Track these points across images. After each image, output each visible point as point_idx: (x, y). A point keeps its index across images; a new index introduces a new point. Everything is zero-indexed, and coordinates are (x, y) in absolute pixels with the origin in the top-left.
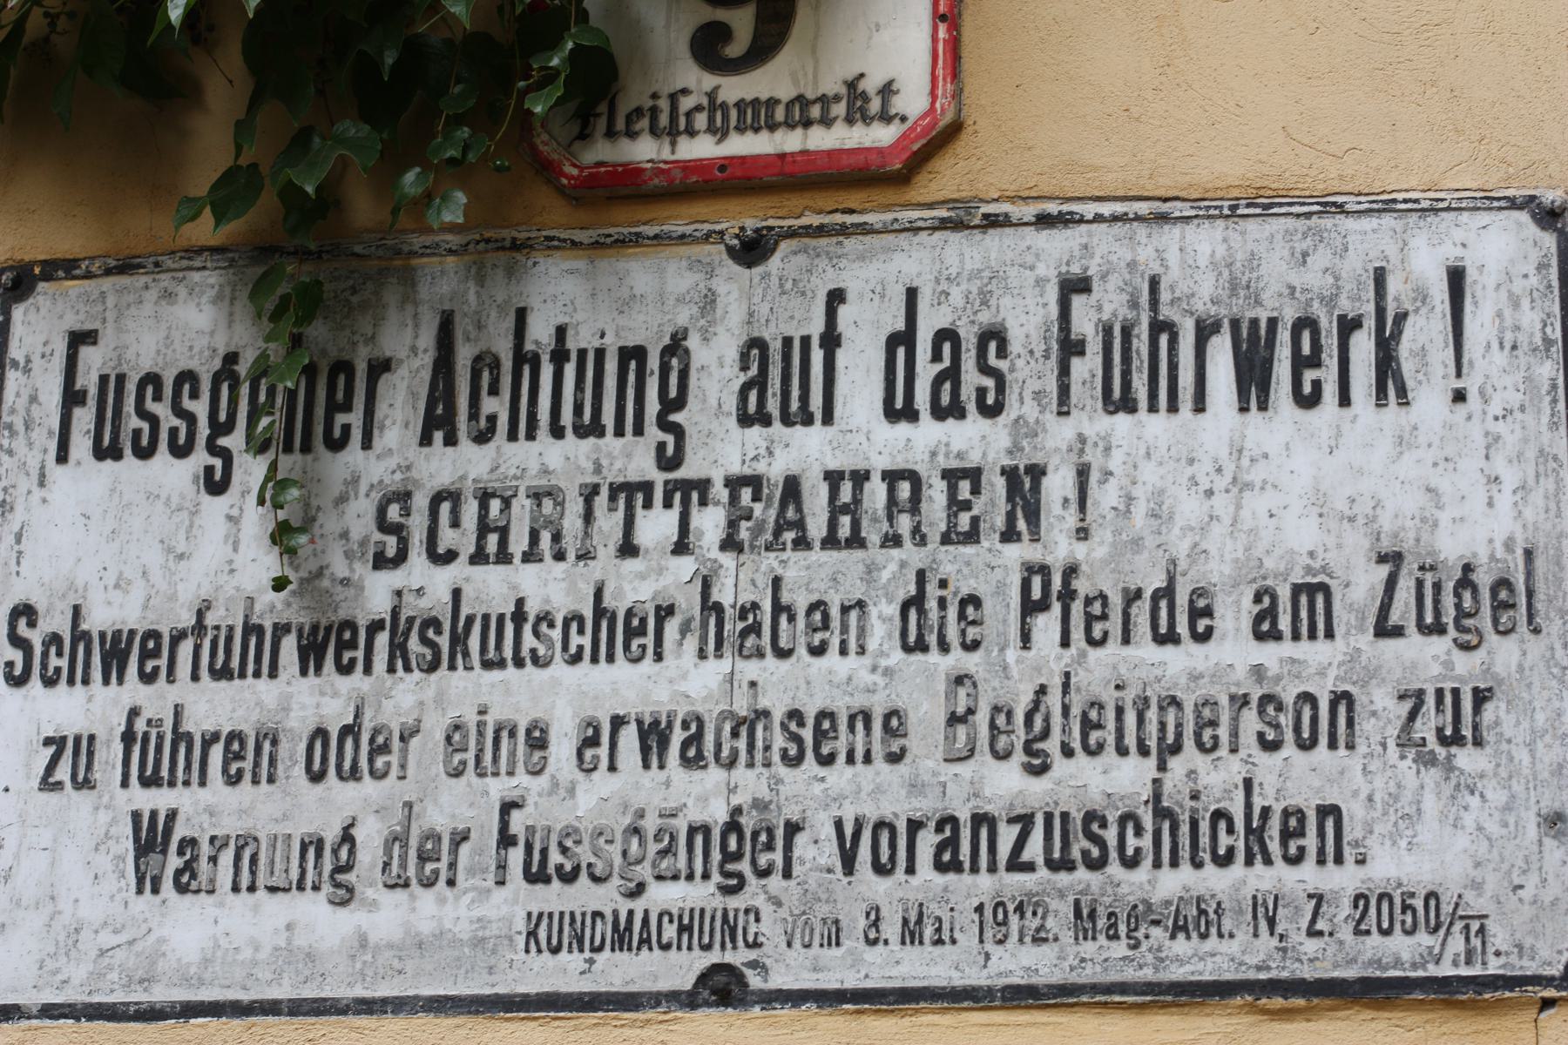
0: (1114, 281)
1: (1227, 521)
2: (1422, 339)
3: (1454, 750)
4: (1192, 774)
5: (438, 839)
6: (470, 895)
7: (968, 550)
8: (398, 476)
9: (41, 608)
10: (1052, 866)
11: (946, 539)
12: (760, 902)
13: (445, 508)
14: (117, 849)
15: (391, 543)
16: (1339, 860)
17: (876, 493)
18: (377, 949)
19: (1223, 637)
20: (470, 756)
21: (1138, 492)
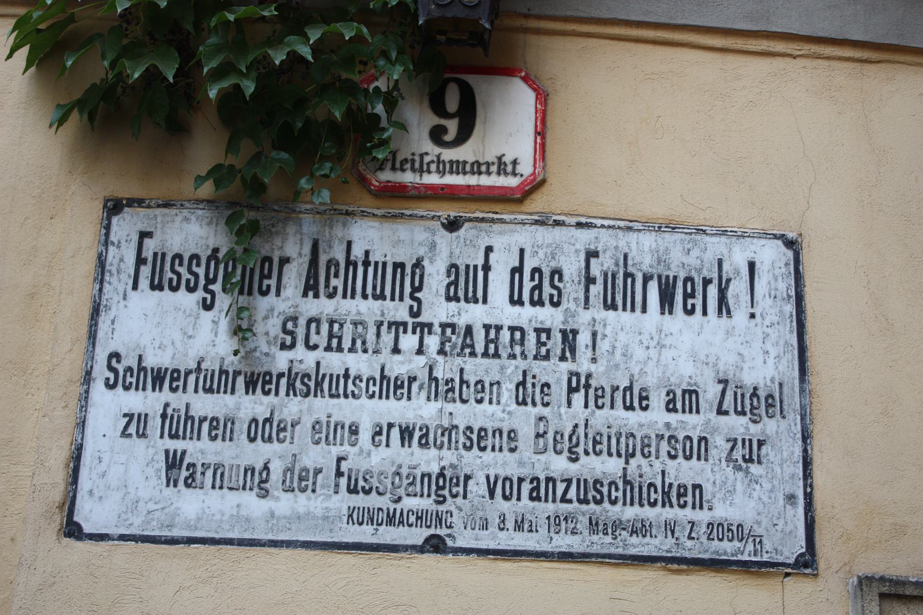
0: (609, 254)
1: (655, 360)
2: (737, 290)
3: (749, 465)
4: (639, 466)
5: (308, 471)
6: (322, 497)
7: (545, 363)
8: (292, 310)
9: (123, 354)
10: (580, 501)
11: (535, 358)
12: (453, 508)
13: (313, 325)
14: (157, 466)
15: (288, 339)
16: (701, 507)
17: (505, 335)
18: (279, 519)
19: (653, 409)
20: (323, 436)
21: (617, 344)
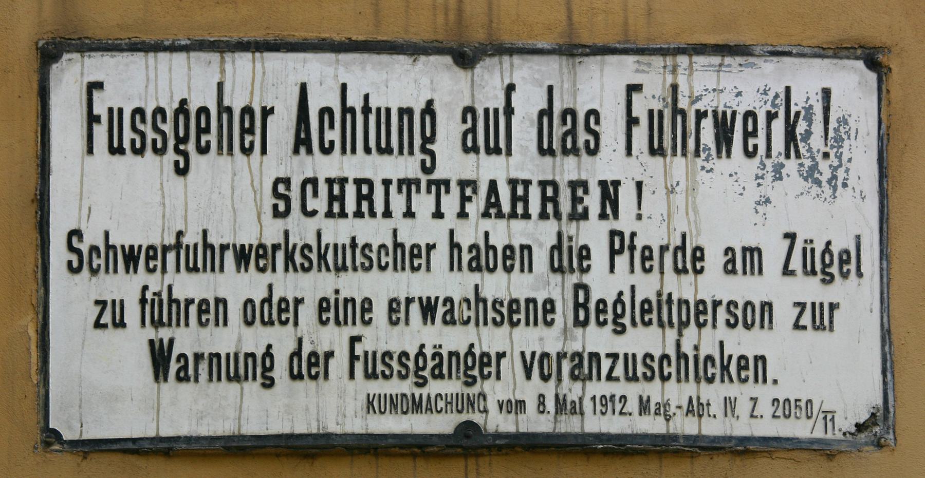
10: (628, 379)
13: (309, 188)
